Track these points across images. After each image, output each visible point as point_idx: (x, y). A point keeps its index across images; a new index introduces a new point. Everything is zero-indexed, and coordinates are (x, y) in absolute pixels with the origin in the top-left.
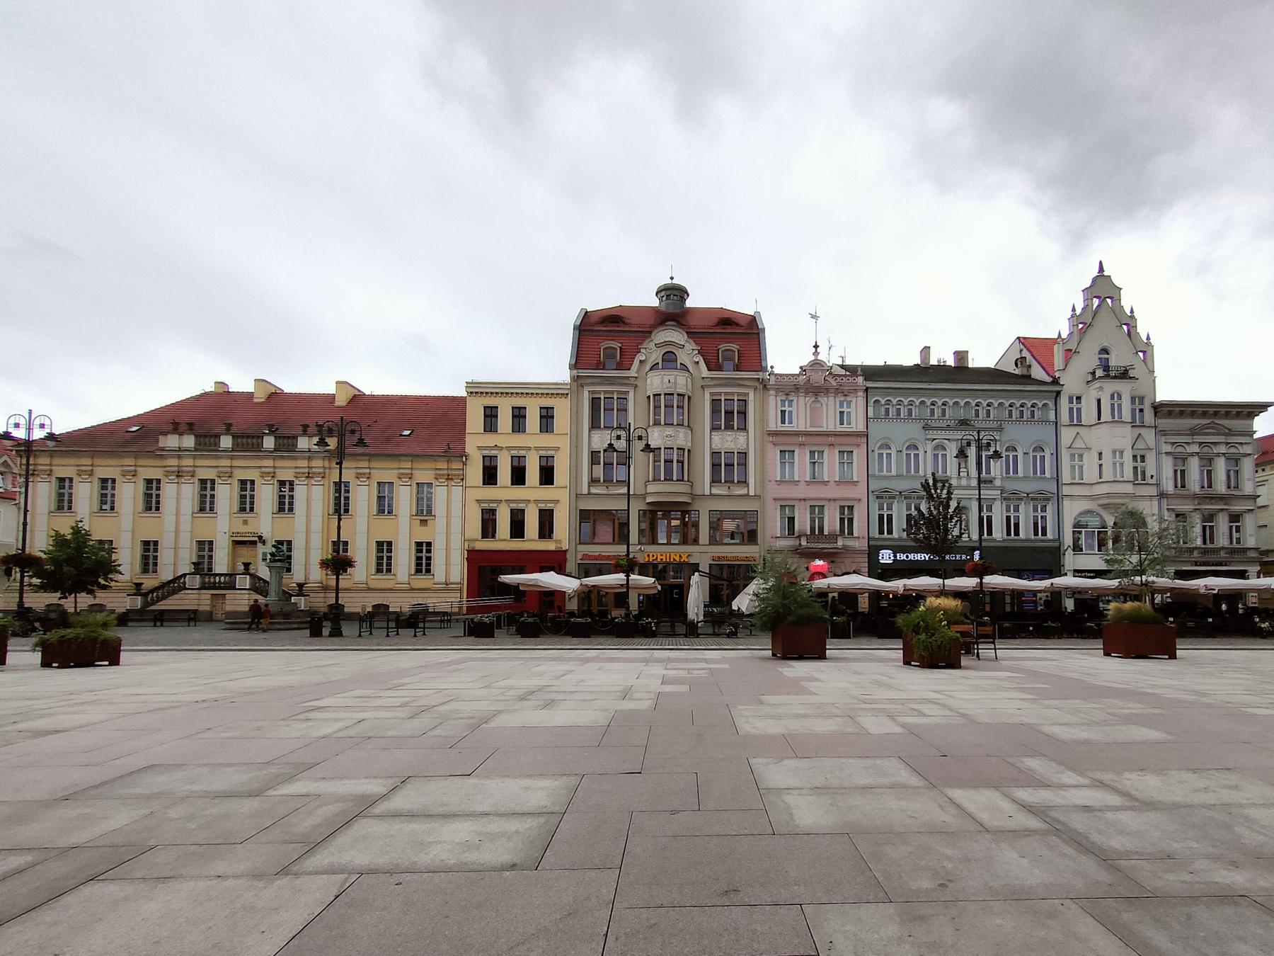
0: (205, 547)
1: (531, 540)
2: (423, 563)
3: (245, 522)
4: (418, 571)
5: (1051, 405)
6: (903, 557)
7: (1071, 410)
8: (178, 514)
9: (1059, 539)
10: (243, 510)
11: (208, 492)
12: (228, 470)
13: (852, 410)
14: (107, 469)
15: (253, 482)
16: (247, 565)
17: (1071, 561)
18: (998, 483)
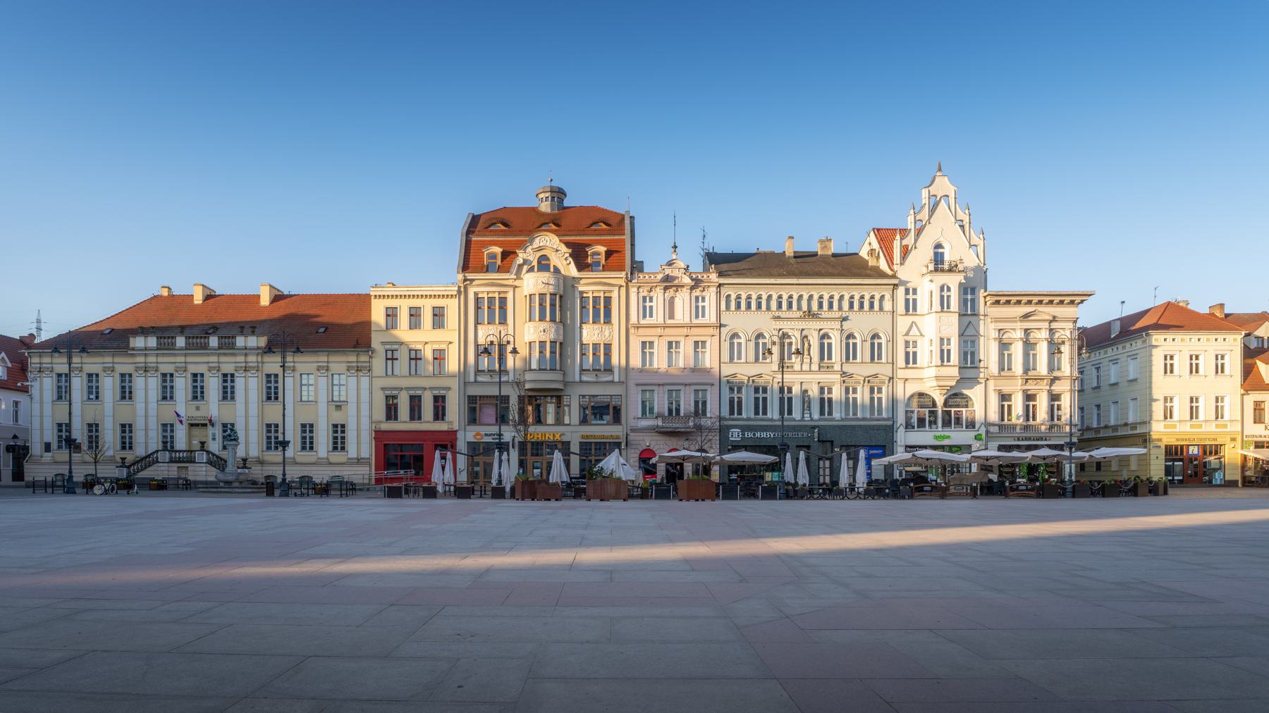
0: (167, 428)
1: (427, 423)
2: (338, 443)
3: (198, 408)
4: (335, 448)
5: (888, 296)
6: (751, 435)
7: (907, 301)
8: (146, 402)
9: (893, 418)
10: (195, 398)
11: (168, 384)
12: (184, 363)
13: (706, 304)
14: (92, 364)
15: (202, 375)
16: (203, 443)
17: (903, 437)
18: (837, 367)
